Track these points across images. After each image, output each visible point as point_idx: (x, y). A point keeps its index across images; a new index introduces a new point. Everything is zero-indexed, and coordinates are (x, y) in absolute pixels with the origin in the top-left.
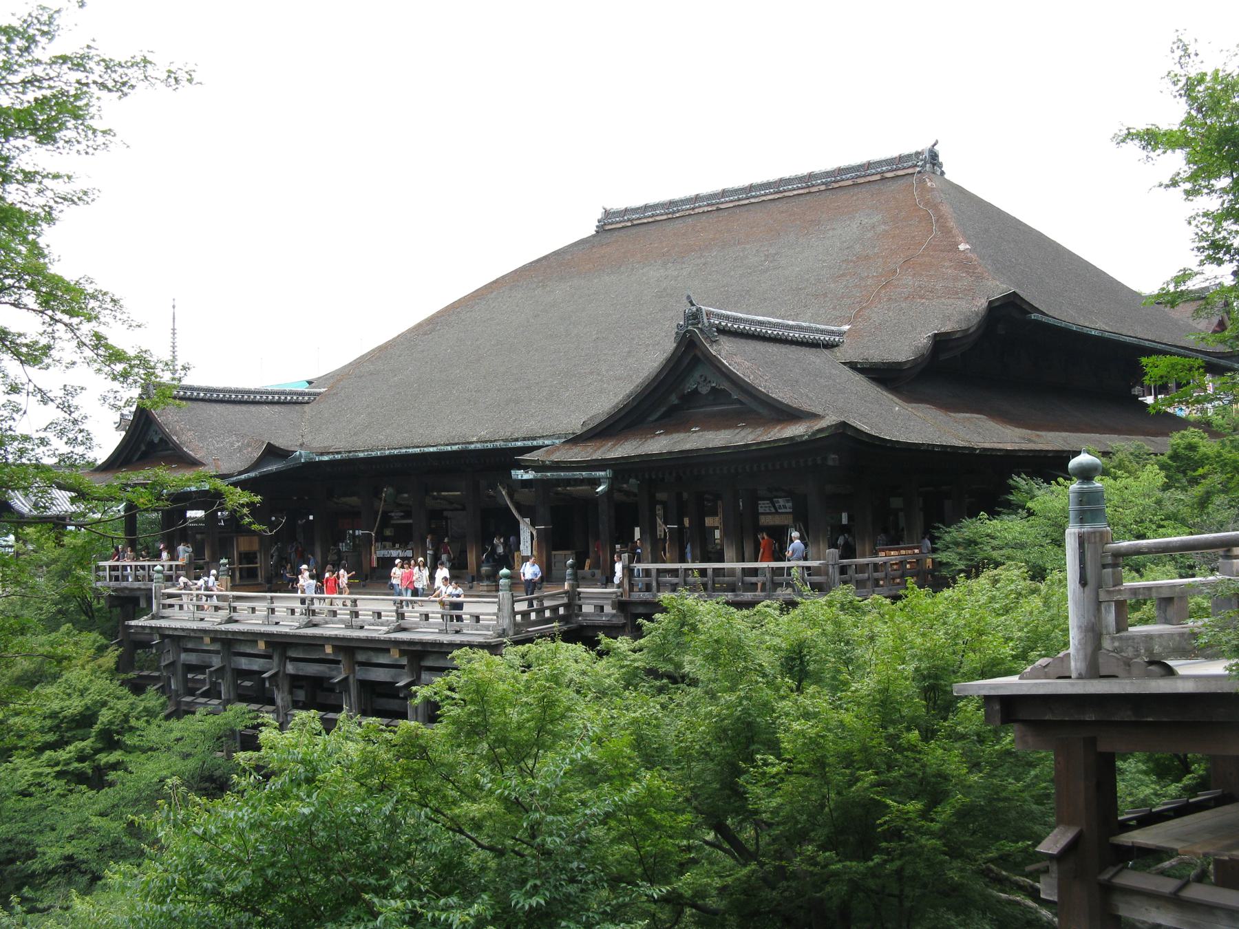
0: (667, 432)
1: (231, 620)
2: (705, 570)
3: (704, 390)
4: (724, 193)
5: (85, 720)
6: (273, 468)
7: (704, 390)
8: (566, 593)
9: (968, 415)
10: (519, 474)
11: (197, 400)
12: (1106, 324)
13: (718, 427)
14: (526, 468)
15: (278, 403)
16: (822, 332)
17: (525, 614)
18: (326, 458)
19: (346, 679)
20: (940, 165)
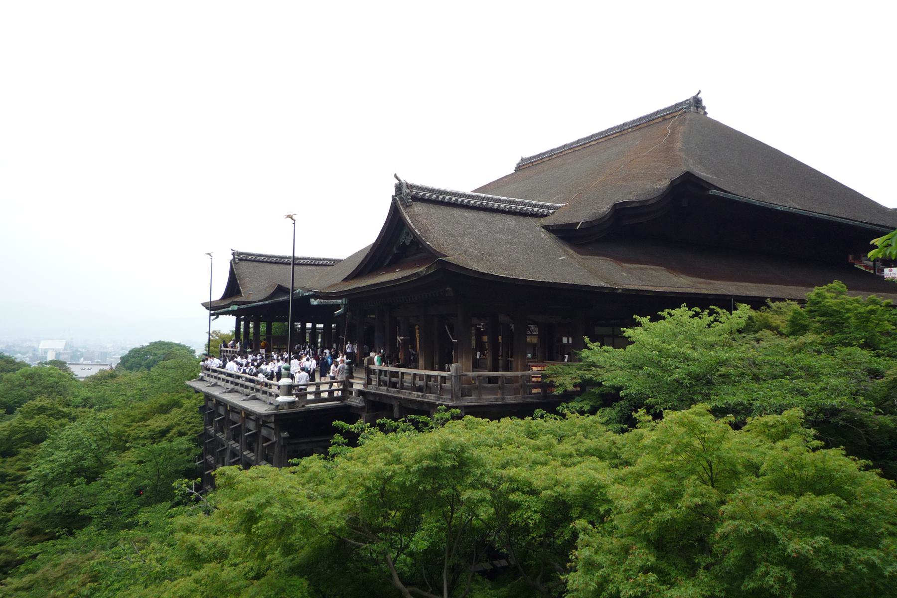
0: (387, 272)
1: (215, 385)
2: (397, 372)
3: (408, 243)
4: (578, 141)
5: (163, 433)
6: (281, 299)
7: (408, 243)
10: (314, 302)
11: (263, 262)
12: (799, 204)
13: (404, 270)
15: (314, 265)
16: (535, 206)
19: (240, 426)
20: (704, 108)
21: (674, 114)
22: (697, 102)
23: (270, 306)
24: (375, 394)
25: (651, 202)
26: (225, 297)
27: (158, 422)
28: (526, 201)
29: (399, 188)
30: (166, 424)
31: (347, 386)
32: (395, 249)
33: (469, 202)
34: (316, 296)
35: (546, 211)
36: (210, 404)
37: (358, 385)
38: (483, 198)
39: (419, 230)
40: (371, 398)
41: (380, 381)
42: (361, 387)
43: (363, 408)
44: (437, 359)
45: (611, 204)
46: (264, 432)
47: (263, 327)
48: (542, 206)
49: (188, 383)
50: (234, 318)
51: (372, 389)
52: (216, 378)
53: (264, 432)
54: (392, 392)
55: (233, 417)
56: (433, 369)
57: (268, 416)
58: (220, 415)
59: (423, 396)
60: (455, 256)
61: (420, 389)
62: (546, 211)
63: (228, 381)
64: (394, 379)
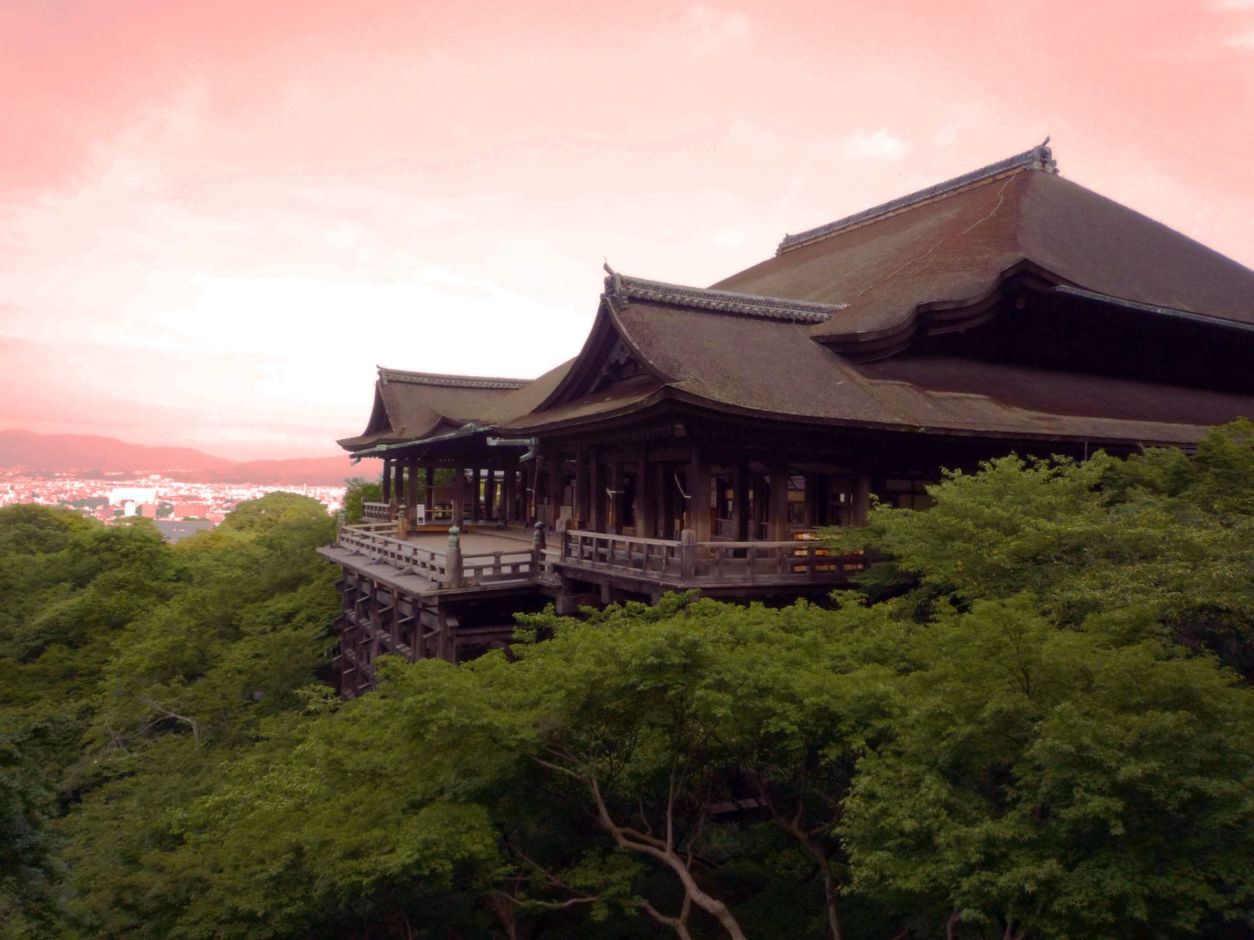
0: (593, 403)
1: (357, 554)
2: (607, 540)
3: (622, 362)
5: (288, 618)
7: (622, 362)
8: (530, 552)
9: (956, 394)
10: (492, 442)
13: (617, 399)
14: (501, 436)
16: (803, 308)
17: (478, 569)
18: (481, 430)
19: (391, 610)
20: (1054, 163)
21: (1009, 173)
22: (1043, 154)
23: (433, 446)
24: (576, 571)
25: (970, 303)
26: (368, 433)
27: (281, 603)
28: (791, 302)
29: (610, 283)
30: (292, 605)
31: (537, 556)
32: (604, 368)
33: (709, 303)
34: (494, 433)
35: (819, 315)
36: (350, 580)
37: (553, 554)
38: (729, 298)
39: (639, 344)
40: (570, 575)
41: (582, 551)
42: (557, 561)
43: (559, 588)
44: (661, 522)
45: (914, 306)
46: (424, 618)
47: (422, 474)
48: (813, 309)
49: (319, 550)
50: (382, 461)
51: (571, 562)
52: (358, 543)
53: (424, 618)
54: (601, 568)
55: (382, 597)
56: (656, 536)
57: (430, 597)
58: (364, 595)
59: (644, 574)
60: (688, 382)
61: (638, 564)
62: (819, 315)
63: (374, 549)
64: (601, 550)
